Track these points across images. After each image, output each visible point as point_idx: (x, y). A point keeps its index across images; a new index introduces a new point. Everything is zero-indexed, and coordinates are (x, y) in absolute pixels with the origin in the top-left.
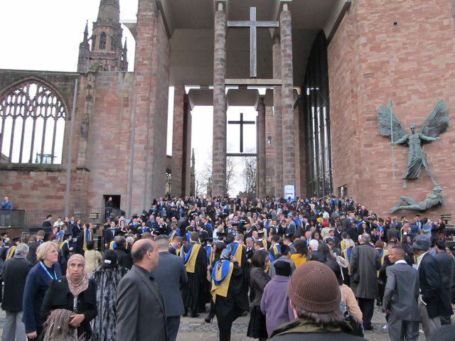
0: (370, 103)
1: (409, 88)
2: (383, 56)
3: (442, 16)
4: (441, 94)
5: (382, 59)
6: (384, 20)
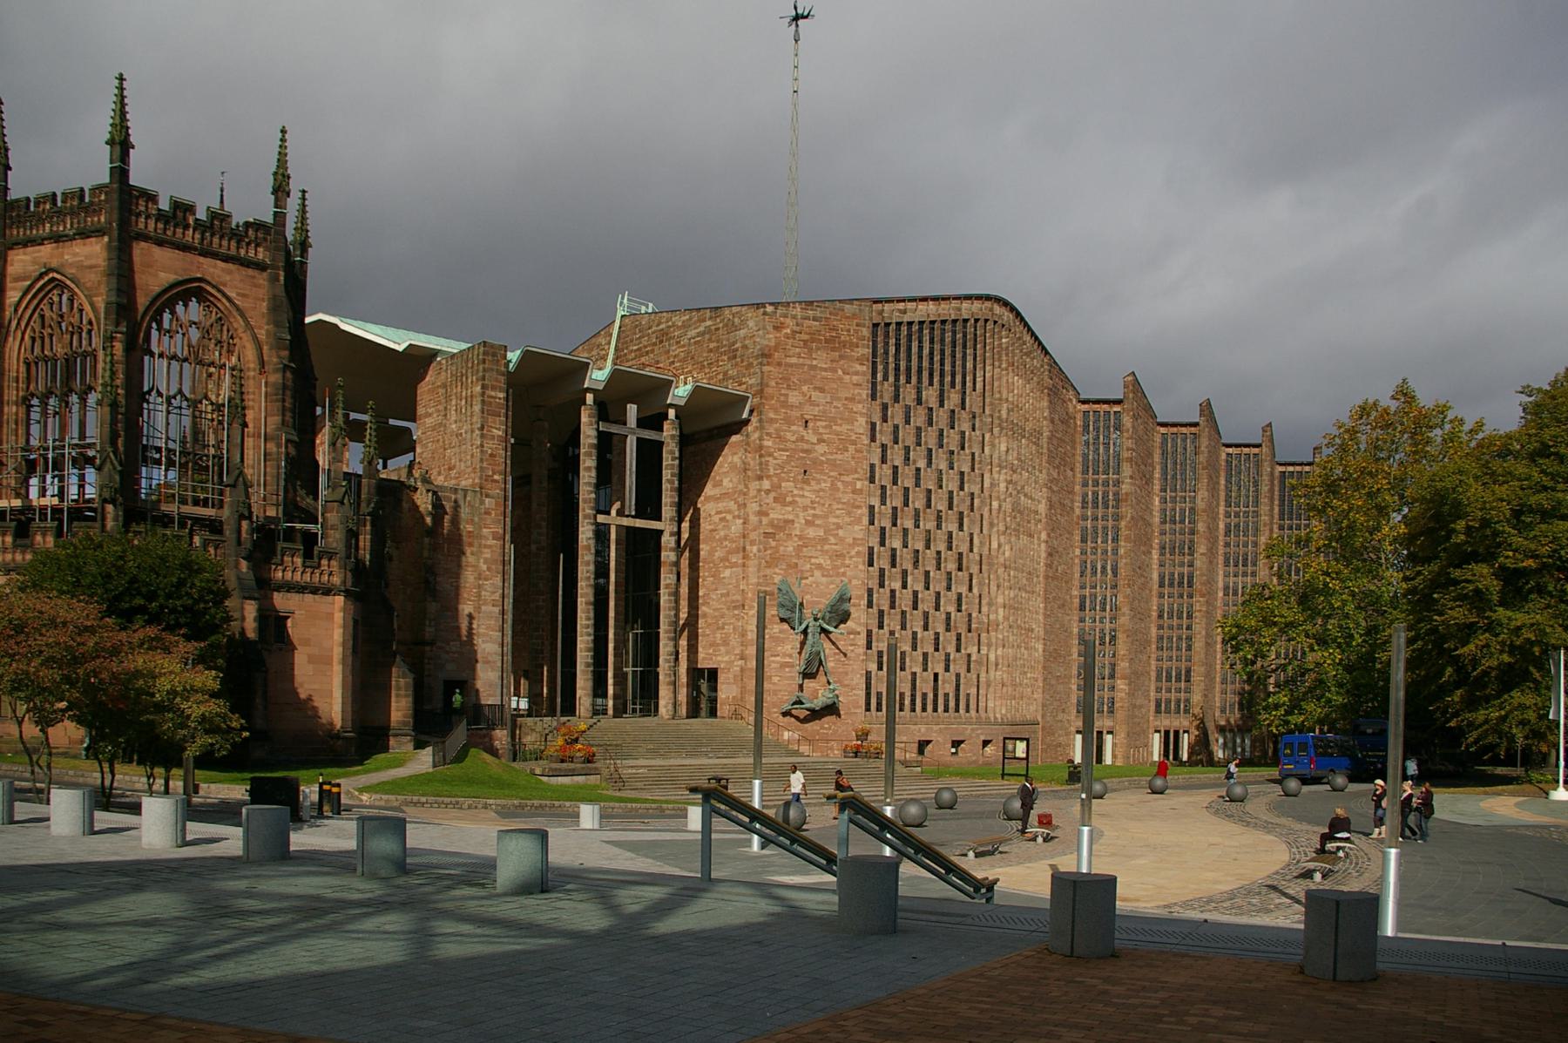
0: (768, 572)
1: (813, 560)
3: (856, 476)
4: (844, 574)
5: (786, 517)
6: (793, 464)
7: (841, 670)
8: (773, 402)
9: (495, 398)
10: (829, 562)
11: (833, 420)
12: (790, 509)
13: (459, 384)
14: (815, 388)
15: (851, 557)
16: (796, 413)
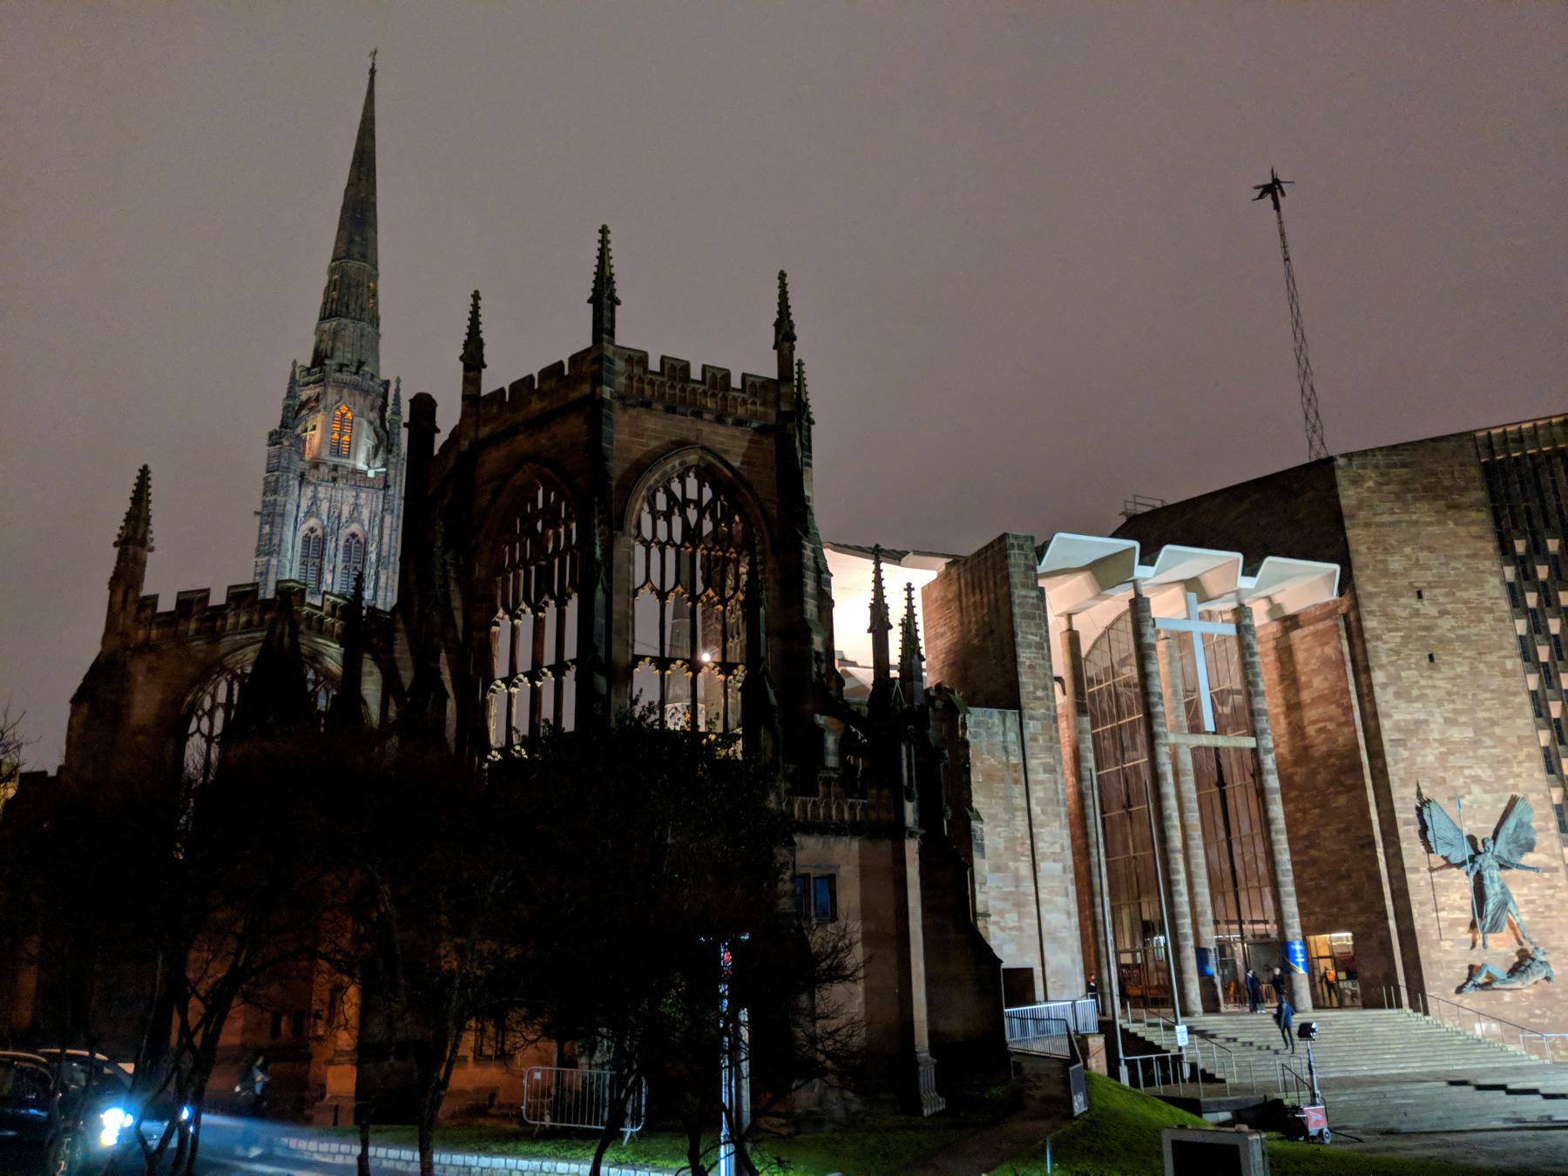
1: (1467, 772)
3: (1503, 653)
4: (1515, 787)
5: (1416, 716)
6: (1411, 646)
7: (1541, 926)
8: (1368, 572)
9: (1025, 597)
10: (1489, 772)
11: (1453, 586)
12: (1418, 705)
13: (977, 591)
14: (1422, 549)
15: (1520, 763)
16: (1401, 582)
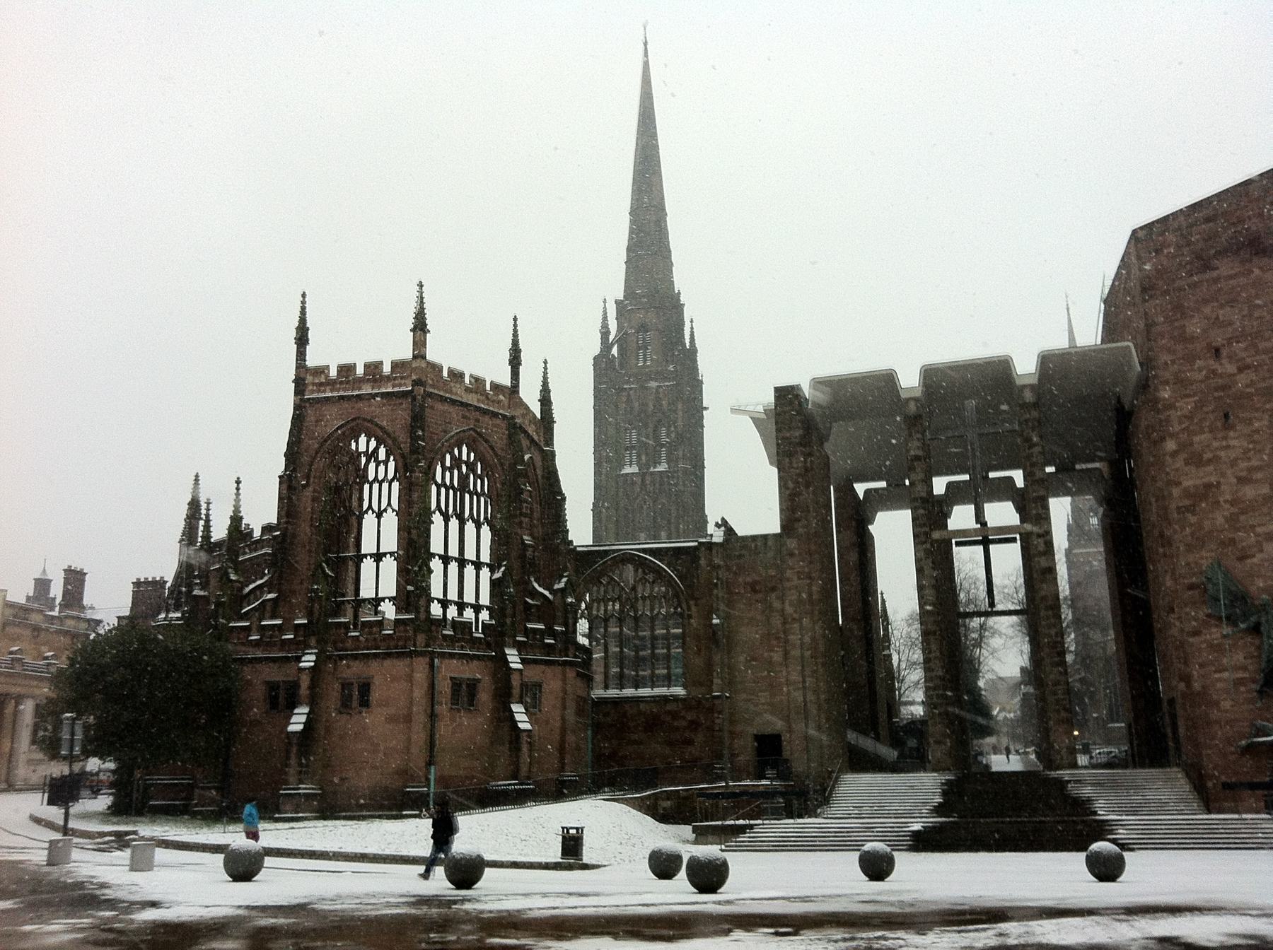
0: (1191, 558)
1: (1259, 530)
2: (1208, 475)
5: (1206, 480)
12: (1211, 468)
14: (1222, 307)
